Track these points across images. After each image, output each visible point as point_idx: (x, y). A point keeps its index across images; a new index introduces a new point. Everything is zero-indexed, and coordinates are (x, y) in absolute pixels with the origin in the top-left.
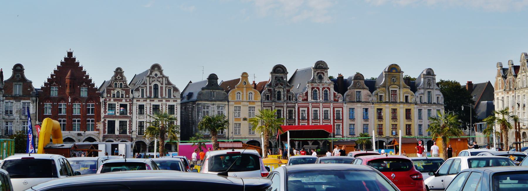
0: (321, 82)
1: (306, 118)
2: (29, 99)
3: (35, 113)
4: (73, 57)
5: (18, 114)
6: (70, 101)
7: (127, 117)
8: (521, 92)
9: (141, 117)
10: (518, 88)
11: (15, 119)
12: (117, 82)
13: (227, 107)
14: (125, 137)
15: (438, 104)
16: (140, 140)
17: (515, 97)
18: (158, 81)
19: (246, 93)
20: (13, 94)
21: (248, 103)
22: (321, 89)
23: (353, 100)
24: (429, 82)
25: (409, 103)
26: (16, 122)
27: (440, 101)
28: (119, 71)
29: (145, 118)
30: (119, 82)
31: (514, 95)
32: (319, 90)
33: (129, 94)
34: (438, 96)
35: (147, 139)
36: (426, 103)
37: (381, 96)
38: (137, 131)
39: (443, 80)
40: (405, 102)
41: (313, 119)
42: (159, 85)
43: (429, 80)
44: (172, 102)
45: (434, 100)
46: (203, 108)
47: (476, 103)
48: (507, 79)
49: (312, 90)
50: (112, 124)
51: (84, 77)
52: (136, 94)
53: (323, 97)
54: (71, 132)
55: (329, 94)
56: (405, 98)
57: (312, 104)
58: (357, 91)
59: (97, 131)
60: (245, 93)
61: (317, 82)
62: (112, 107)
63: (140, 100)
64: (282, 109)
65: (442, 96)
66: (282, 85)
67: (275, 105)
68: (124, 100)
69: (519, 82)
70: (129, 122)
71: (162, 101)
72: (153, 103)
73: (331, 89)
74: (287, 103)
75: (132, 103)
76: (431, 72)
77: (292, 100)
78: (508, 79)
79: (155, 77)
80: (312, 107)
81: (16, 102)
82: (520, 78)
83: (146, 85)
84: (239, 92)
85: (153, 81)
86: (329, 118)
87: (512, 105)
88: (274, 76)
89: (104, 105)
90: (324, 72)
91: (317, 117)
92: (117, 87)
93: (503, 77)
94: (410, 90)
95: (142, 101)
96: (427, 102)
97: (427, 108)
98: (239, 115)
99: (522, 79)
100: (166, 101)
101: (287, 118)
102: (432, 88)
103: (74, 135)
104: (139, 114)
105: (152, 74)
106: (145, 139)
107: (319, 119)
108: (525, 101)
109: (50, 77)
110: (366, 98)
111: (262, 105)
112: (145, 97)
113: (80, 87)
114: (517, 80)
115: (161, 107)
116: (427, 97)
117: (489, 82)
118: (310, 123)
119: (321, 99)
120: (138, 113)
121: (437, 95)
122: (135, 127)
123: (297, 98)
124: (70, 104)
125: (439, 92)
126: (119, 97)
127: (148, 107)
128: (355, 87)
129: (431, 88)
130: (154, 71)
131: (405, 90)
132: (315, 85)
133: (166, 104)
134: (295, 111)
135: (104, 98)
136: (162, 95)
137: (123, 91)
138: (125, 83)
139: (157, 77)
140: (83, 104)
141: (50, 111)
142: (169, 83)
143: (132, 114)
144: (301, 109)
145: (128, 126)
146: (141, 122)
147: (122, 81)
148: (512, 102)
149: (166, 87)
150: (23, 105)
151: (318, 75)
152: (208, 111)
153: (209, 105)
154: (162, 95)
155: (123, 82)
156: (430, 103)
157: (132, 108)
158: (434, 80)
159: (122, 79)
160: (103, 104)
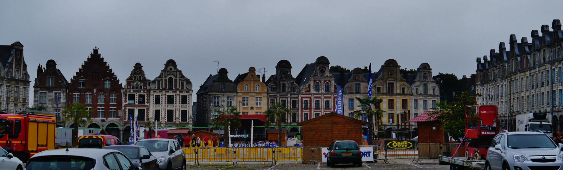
0: (322, 76)
1: (309, 107)
2: (60, 90)
3: (64, 102)
4: (99, 54)
5: (50, 103)
6: (95, 92)
7: (145, 106)
9: (157, 105)
11: (48, 107)
12: (137, 75)
13: (236, 97)
14: (142, 123)
15: (434, 95)
18: (172, 74)
19: (254, 85)
20: (47, 85)
21: (255, 94)
22: (322, 81)
23: (353, 92)
25: (405, 94)
26: (49, 109)
27: (436, 93)
28: (138, 66)
29: (161, 107)
30: (138, 75)
32: (321, 83)
33: (147, 86)
34: (434, 88)
36: (422, 94)
37: (379, 89)
38: (153, 118)
39: (441, 73)
40: (401, 93)
41: (315, 108)
42: (174, 78)
43: (425, 73)
45: (430, 91)
46: (214, 98)
49: (314, 83)
50: (131, 112)
51: (108, 71)
52: (153, 86)
53: (325, 89)
54: (96, 118)
55: (330, 86)
56: (401, 89)
57: (314, 95)
58: (356, 84)
59: (119, 118)
60: (252, 86)
61: (319, 76)
62: (132, 97)
64: (287, 99)
65: (437, 88)
66: (286, 78)
67: (280, 96)
68: (142, 91)
70: (147, 110)
71: (176, 92)
72: (168, 94)
73: (332, 81)
74: (291, 94)
75: (149, 94)
76: (427, 67)
77: (296, 92)
79: (170, 71)
80: (314, 98)
81: (48, 92)
84: (247, 84)
85: (168, 75)
86: (330, 107)
88: (279, 70)
89: (125, 95)
90: (326, 67)
91: (319, 107)
92: (136, 80)
94: (406, 82)
95: (158, 92)
96: (423, 94)
97: (423, 98)
98: (247, 105)
100: (180, 92)
101: (290, 107)
102: (428, 80)
103: (98, 121)
107: (320, 108)
109: (78, 71)
110: (365, 90)
111: (267, 96)
112: (161, 88)
113: (78, 79)
118: (312, 112)
119: (323, 91)
120: (154, 102)
121: (432, 87)
122: (152, 115)
123: (301, 90)
124: (96, 94)
125: (434, 85)
126: (138, 89)
127: (164, 97)
128: (354, 80)
129: (427, 80)
131: (402, 83)
132: (317, 78)
134: (298, 101)
135: (124, 90)
136: (176, 87)
137: (141, 83)
138: (143, 76)
139: (172, 71)
140: (107, 94)
141: (91, 100)
142: (182, 76)
144: (304, 99)
145: (145, 113)
147: (141, 75)
149: (179, 80)
150: (55, 95)
151: (320, 69)
152: (219, 101)
153: (219, 96)
154: (176, 87)
155: (142, 75)
156: (426, 94)
157: (149, 98)
158: (430, 74)
159: (141, 73)
160: (124, 94)
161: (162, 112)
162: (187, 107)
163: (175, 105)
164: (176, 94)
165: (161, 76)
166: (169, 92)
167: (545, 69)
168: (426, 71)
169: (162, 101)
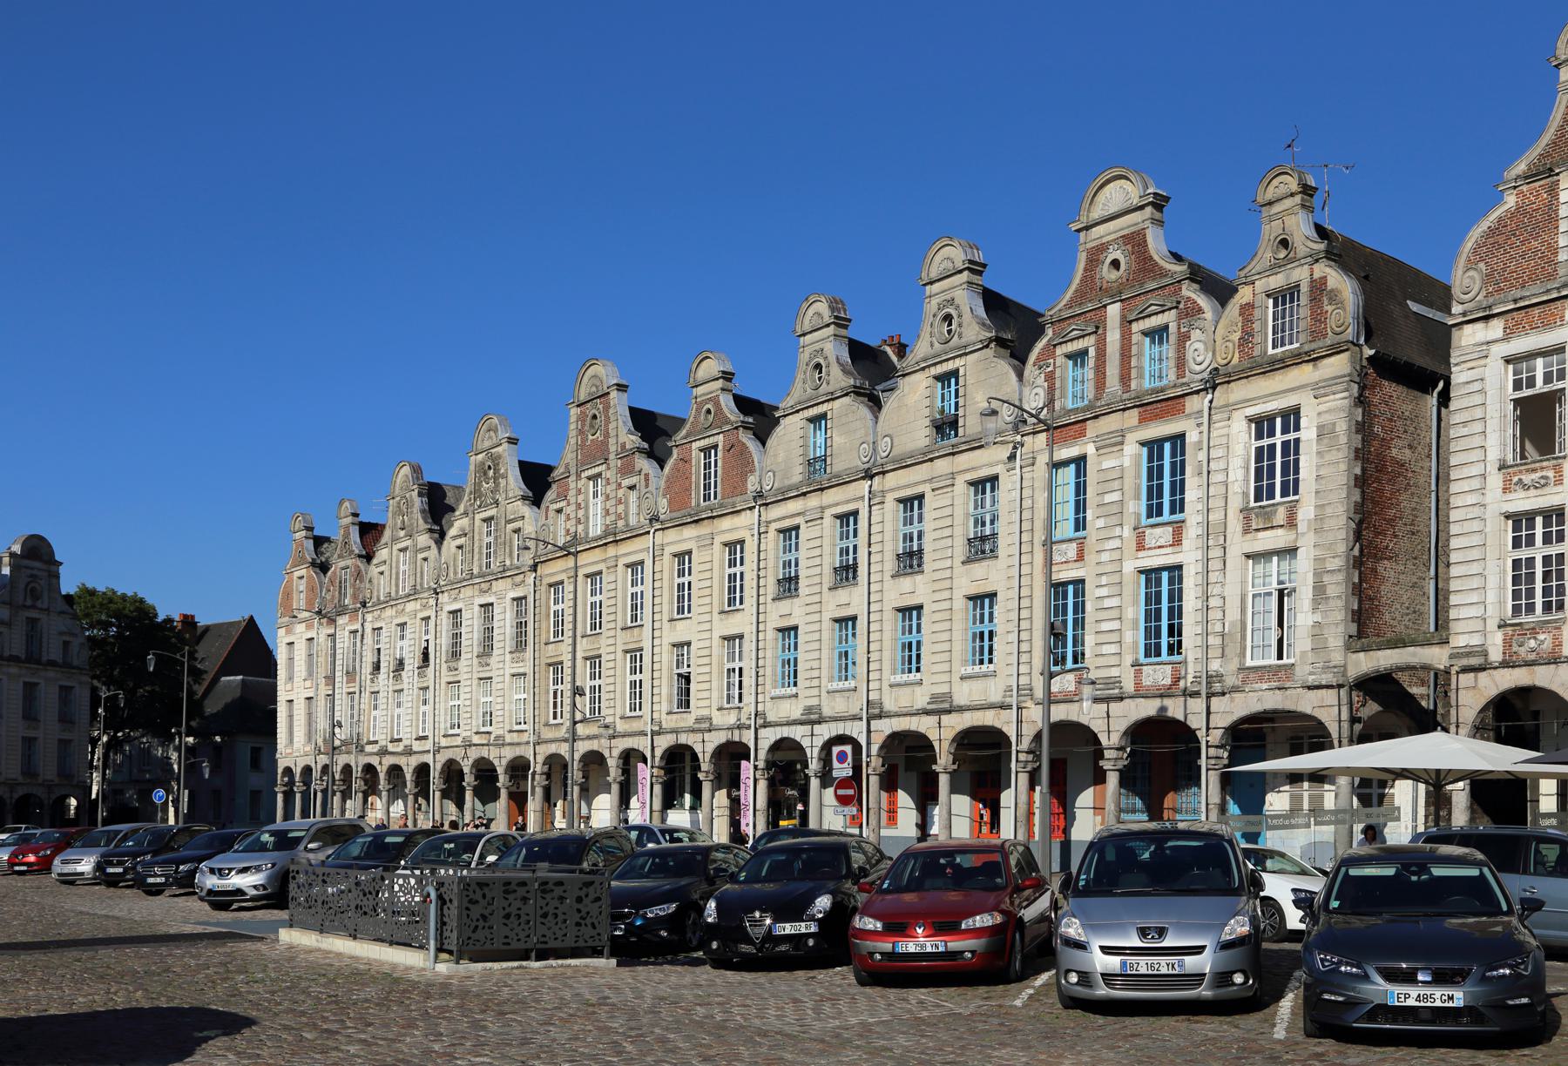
8: (389, 612)
10: (374, 600)
15: (66, 665)
17: (363, 635)
24: (32, 585)
31: (357, 626)
34: (67, 638)
45: (53, 651)
47: (208, 678)
48: (329, 573)
69: (379, 579)
78: (334, 573)
82: (385, 562)
87: (347, 665)
93: (313, 564)
96: (23, 657)
99: (394, 565)
102: (45, 606)
108: (402, 648)
114: (373, 570)
116: (24, 638)
117: (252, 619)
148: (348, 653)
156: (32, 658)
158: (54, 581)
167: (953, 475)
168: (39, 569)
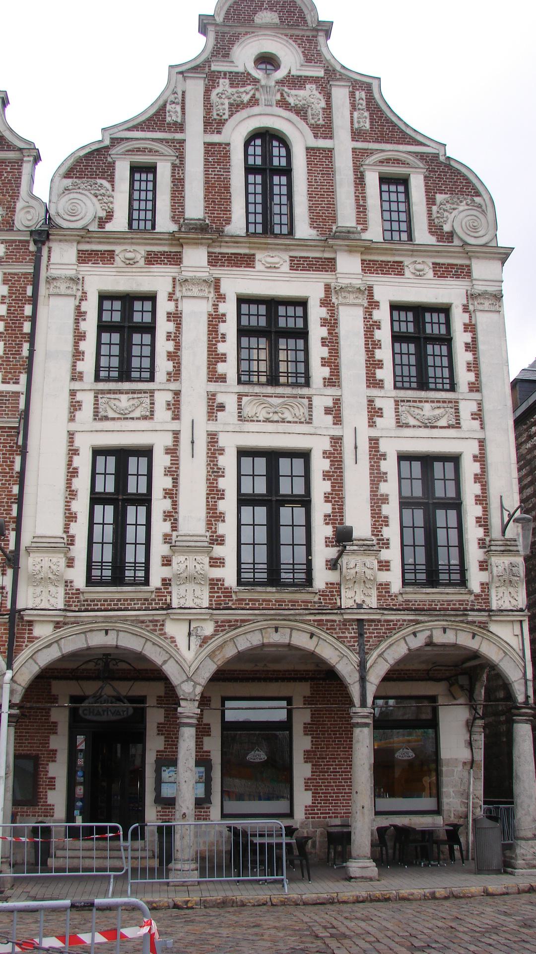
9: (124, 401)
16: (110, 640)
18: (283, 104)
29: (162, 414)
35: (176, 630)
38: (71, 540)
44: (419, 274)
63: (118, 249)
71: (329, 265)
79: (257, 74)
83: (178, 136)
85: (236, 107)
100: (368, 267)
104: (97, 379)
105: (227, 55)
106: (158, 626)
112: (165, 223)
115: (324, 322)
120: (87, 366)
130: (246, 33)
133: (371, 295)
143: (23, 378)
146: (122, 454)
149: (359, 156)
157: (33, 319)
161: (173, 472)
162: (457, 425)
163: (321, 402)
164: (328, 288)
165: (173, 114)
166: (259, 266)
169: (174, 357)
